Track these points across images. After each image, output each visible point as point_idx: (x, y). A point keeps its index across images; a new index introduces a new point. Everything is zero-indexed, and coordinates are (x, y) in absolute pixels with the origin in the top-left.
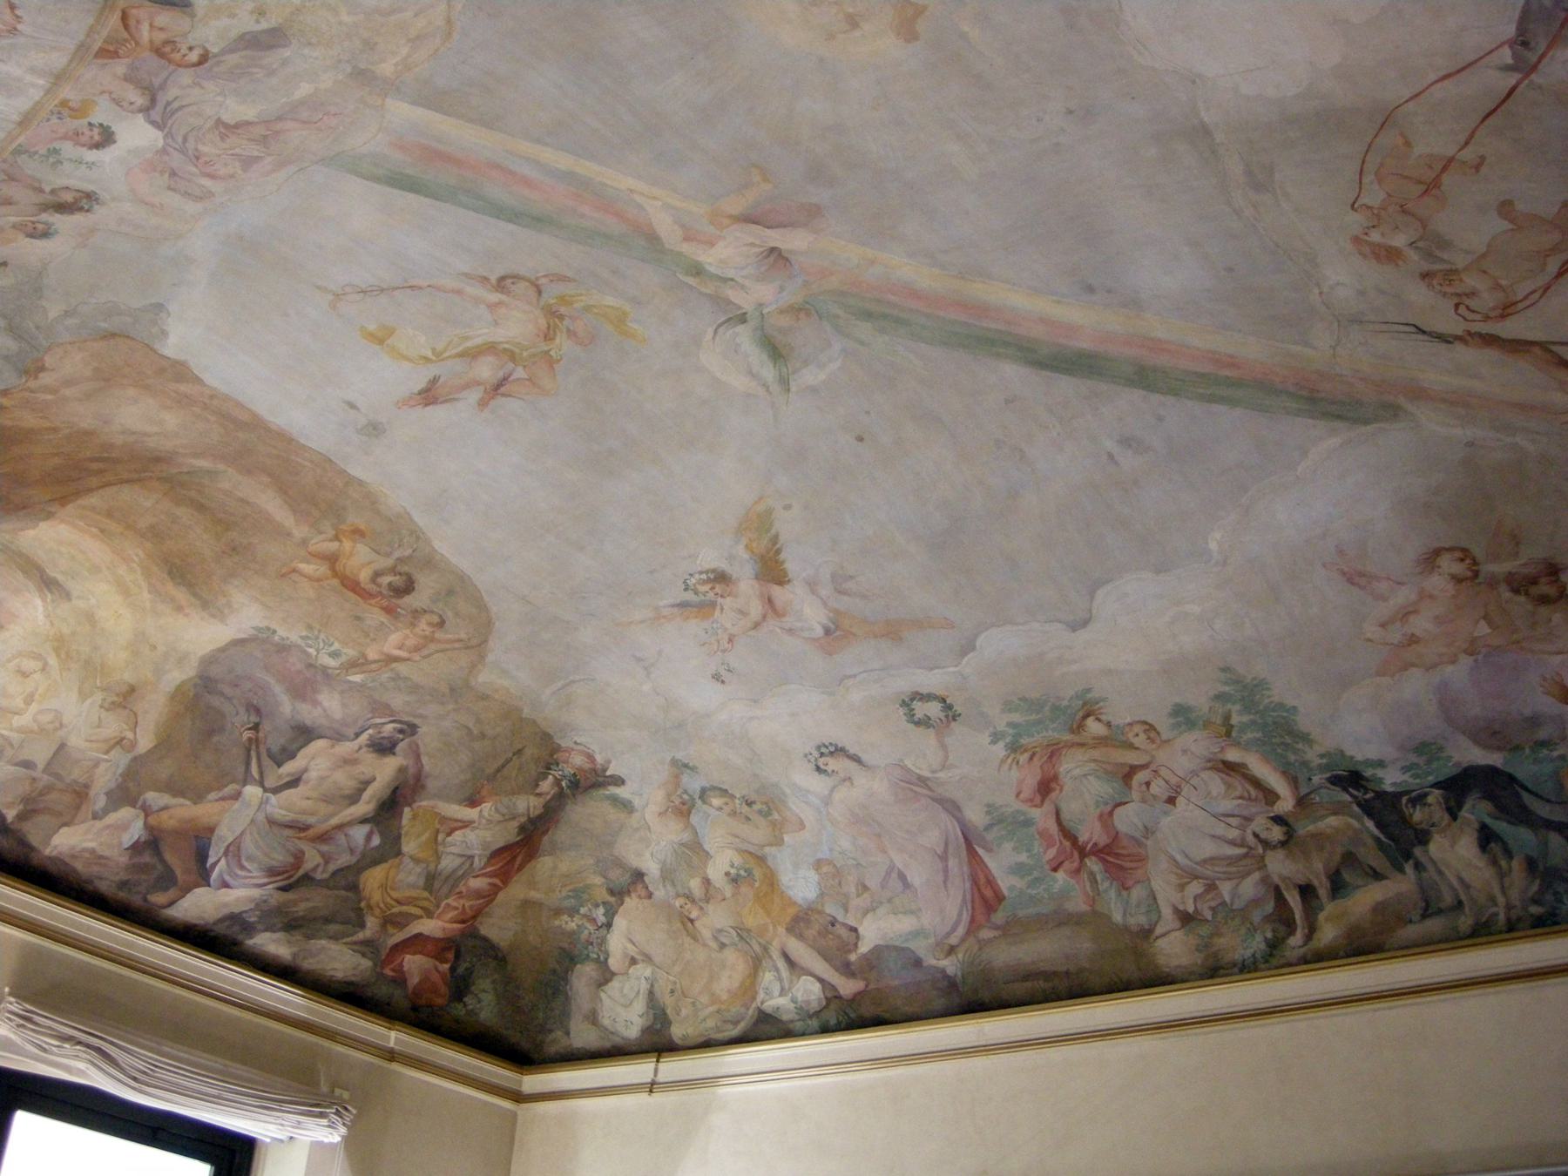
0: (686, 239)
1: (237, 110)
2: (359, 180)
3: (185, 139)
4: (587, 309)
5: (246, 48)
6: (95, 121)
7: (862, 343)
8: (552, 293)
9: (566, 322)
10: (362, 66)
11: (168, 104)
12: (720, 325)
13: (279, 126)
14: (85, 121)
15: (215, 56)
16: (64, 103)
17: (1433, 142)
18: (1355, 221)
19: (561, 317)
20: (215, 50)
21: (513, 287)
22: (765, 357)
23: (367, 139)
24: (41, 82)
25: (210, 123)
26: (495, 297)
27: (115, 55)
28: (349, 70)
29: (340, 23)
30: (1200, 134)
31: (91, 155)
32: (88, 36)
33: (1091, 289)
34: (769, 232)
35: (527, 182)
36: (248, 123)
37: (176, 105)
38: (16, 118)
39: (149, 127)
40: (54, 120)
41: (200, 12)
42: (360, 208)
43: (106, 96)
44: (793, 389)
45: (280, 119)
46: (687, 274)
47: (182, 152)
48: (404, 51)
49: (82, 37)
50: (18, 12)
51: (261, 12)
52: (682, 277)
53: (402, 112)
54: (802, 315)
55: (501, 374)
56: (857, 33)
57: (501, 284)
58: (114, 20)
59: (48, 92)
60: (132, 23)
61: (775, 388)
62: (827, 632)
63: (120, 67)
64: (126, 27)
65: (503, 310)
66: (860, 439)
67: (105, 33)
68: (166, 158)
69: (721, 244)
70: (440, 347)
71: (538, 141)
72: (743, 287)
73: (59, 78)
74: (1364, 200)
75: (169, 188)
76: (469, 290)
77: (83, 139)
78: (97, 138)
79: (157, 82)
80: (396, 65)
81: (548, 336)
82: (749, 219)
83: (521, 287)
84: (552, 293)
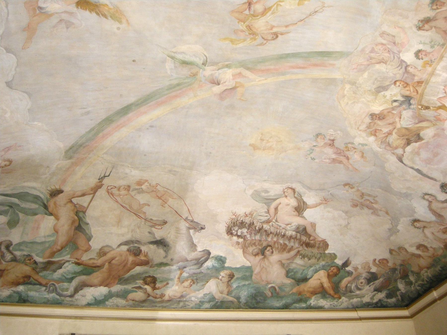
0: (240, 74)
1: (382, 68)
2: (338, 50)
3: (394, 57)
4: (245, 40)
5: (385, 87)
6: (421, 60)
7: (171, 80)
8: (259, 40)
9: (247, 34)
10: (354, 86)
11: (401, 68)
12: (206, 57)
13: (368, 63)
14: (424, 60)
15: (392, 84)
16: (430, 66)
17: (171, 202)
18: (154, 183)
19: (250, 34)
20: (393, 86)
21: (272, 36)
22: (186, 60)
23: (342, 63)
24: (437, 72)
25: (388, 63)
26: (275, 30)
27: (418, 82)
28: (357, 85)
29: (364, 98)
30: (191, 169)
31: (421, 47)
32: (426, 87)
33: (152, 126)
34: (225, 88)
35: (293, 67)
36: (377, 63)
37: (400, 68)
38: (444, 59)
39: (406, 61)
40: (433, 59)
41: (399, 95)
42: (332, 40)
43: (419, 69)
44: (168, 58)
45: (369, 65)
46: (230, 64)
47: (394, 53)
48: (345, 92)
49: (427, 86)
50: (444, 91)
51: (385, 96)
52: (229, 62)
53: (337, 75)
54: (192, 75)
55: (252, 8)
56: (259, 138)
57: (276, 36)
58: (420, 91)
59: (435, 69)
60: (415, 91)
61: (173, 54)
62: (40, 8)
63: (416, 79)
64: (417, 90)
65: (269, 27)
66: (134, 61)
67: (422, 87)
68: (398, 49)
69: (231, 77)
70: (279, 8)
71: (298, 79)
72: (213, 70)
73: (432, 74)
74: (159, 186)
75: (394, 36)
76: (284, 29)
77: (424, 53)
78: (420, 54)
79: (406, 75)
80: (346, 88)
81: (249, 28)
82: (234, 88)
83: (270, 38)
84: (259, 40)
